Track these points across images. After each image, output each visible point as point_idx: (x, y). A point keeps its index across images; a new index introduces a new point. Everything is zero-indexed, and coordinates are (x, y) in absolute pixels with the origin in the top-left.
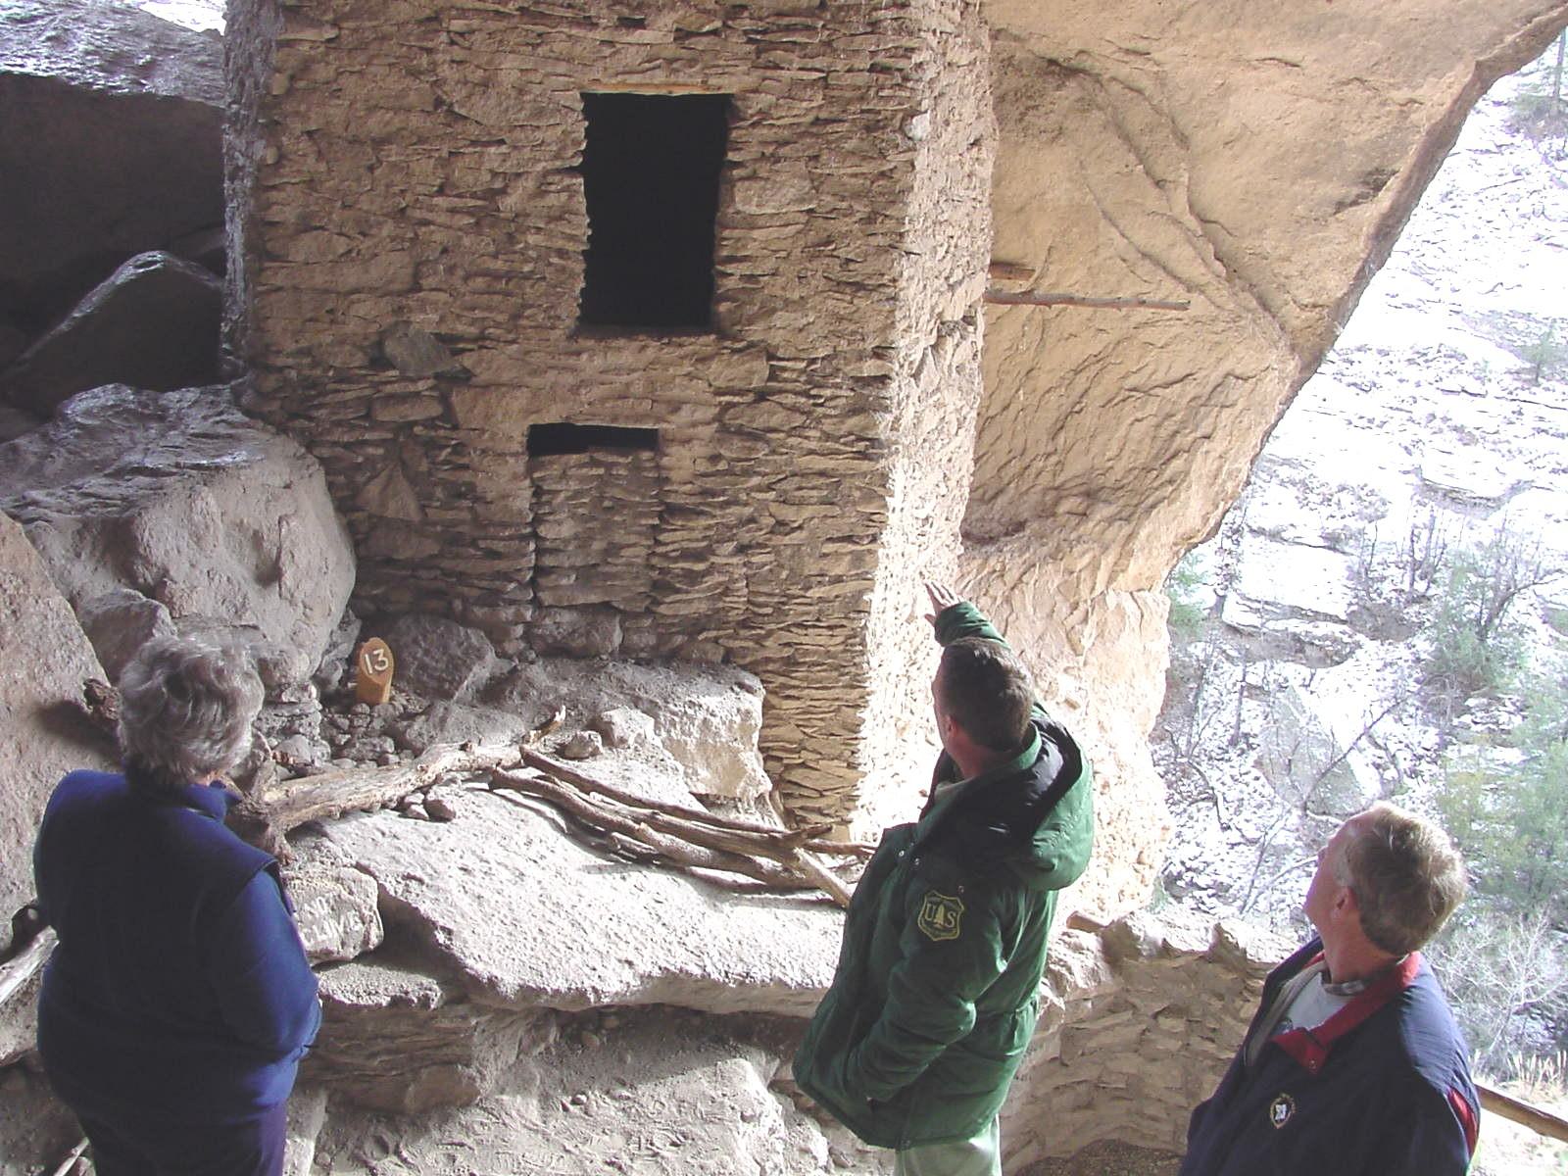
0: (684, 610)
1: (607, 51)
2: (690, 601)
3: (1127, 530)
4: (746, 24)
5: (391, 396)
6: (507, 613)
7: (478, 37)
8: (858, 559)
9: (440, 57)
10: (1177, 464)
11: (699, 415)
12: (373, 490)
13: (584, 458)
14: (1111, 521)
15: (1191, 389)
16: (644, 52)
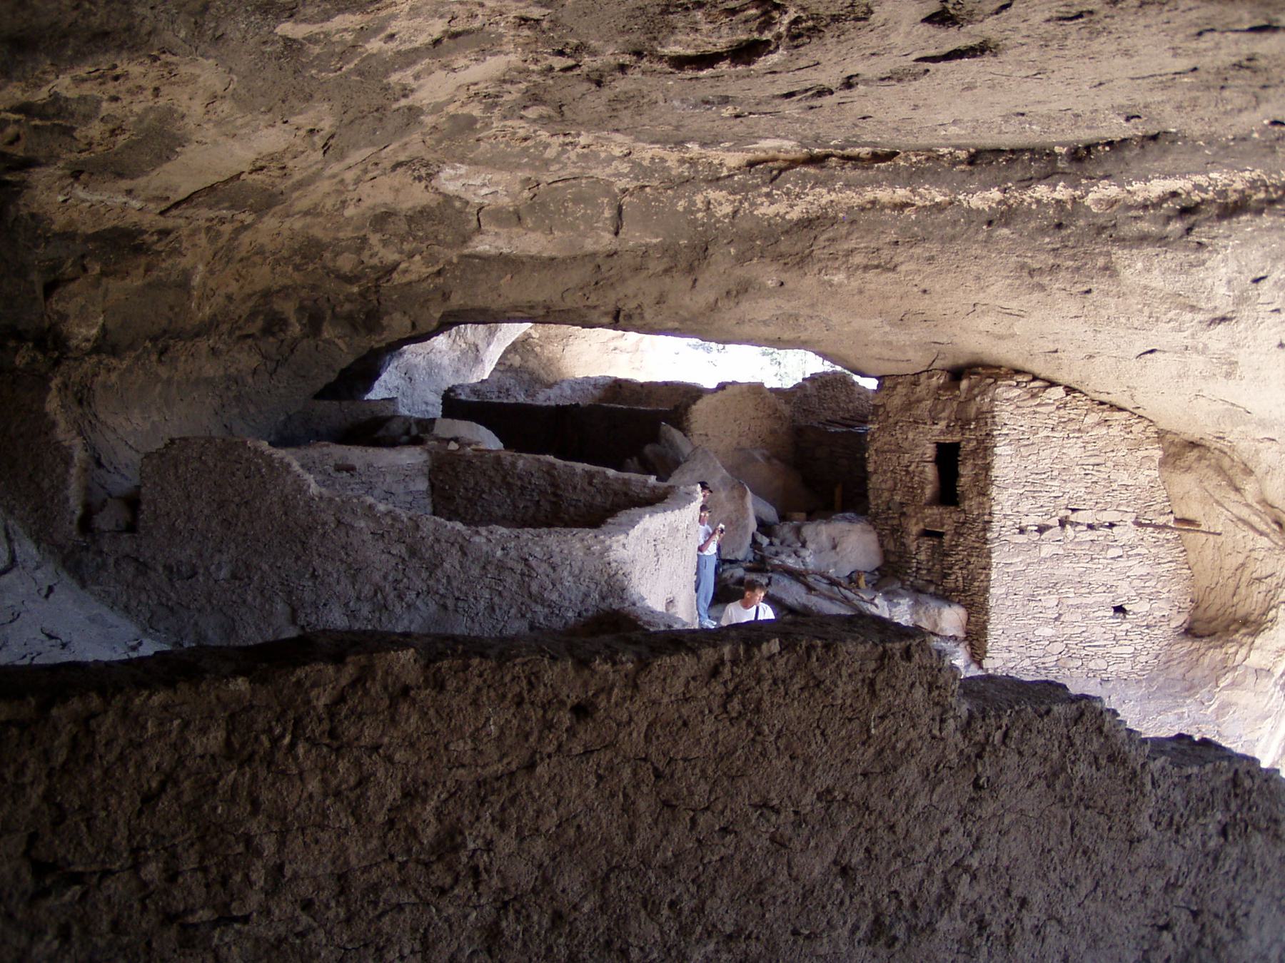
3: (1250, 640)
8: (988, 575)
10: (1272, 614)
14: (1245, 635)
15: (1275, 580)
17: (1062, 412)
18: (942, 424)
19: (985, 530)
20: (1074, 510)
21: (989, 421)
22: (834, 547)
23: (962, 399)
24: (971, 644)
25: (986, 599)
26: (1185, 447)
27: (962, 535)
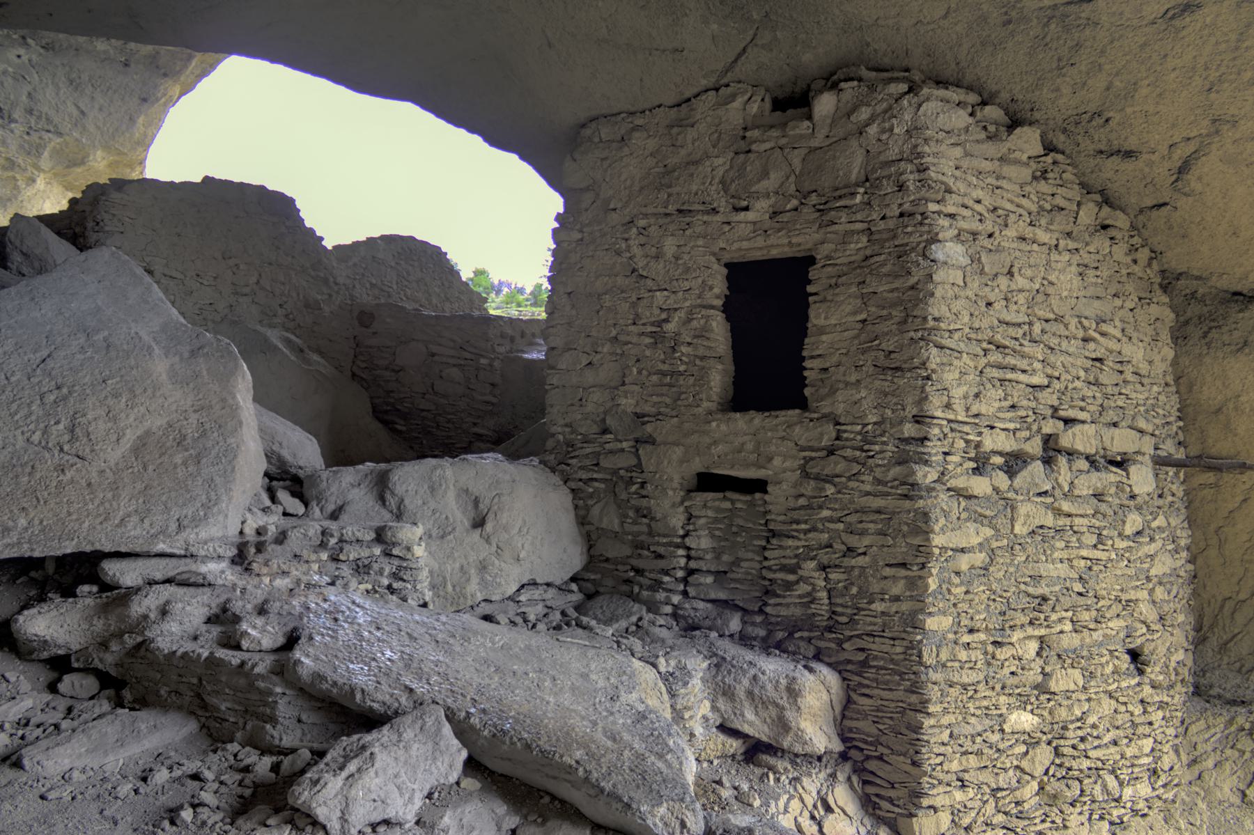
0: (784, 612)
1: (727, 228)
2: (788, 605)
4: (814, 199)
5: (611, 452)
6: (661, 596)
7: (653, 229)
8: (912, 583)
9: (631, 242)
11: (788, 464)
12: (595, 511)
13: (720, 495)
16: (750, 227)
17: (1043, 187)
18: (761, 208)
19: (902, 460)
20: (1068, 422)
21: (911, 179)
22: (479, 523)
23: (815, 143)
24: (859, 770)
25: (913, 650)
26: (1224, 302)
27: (829, 479)
